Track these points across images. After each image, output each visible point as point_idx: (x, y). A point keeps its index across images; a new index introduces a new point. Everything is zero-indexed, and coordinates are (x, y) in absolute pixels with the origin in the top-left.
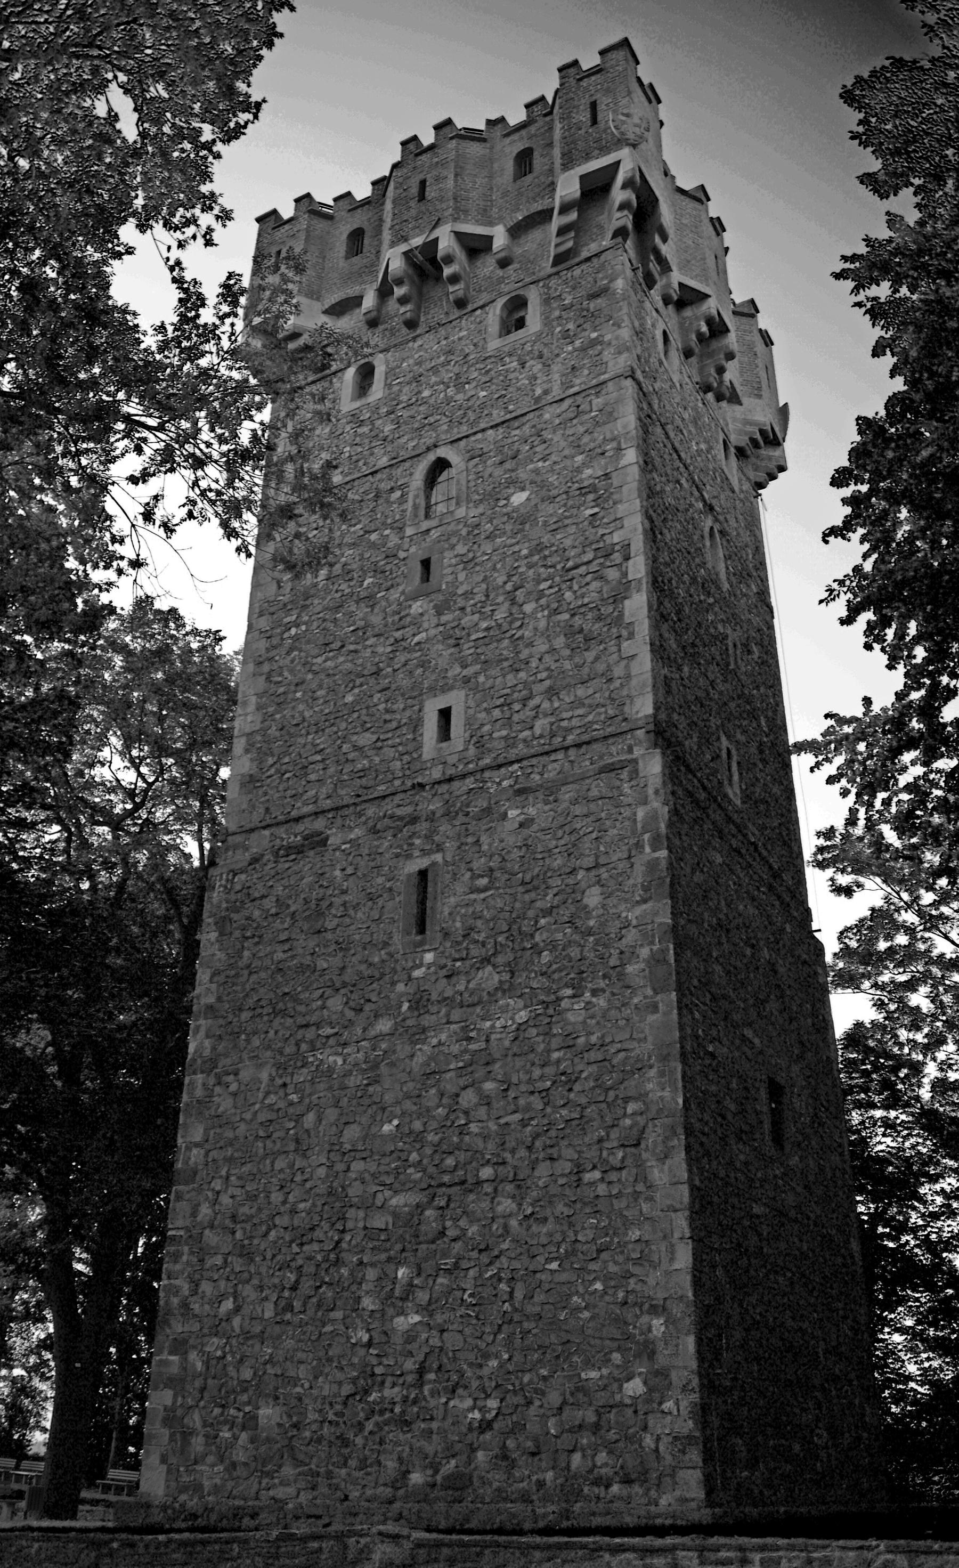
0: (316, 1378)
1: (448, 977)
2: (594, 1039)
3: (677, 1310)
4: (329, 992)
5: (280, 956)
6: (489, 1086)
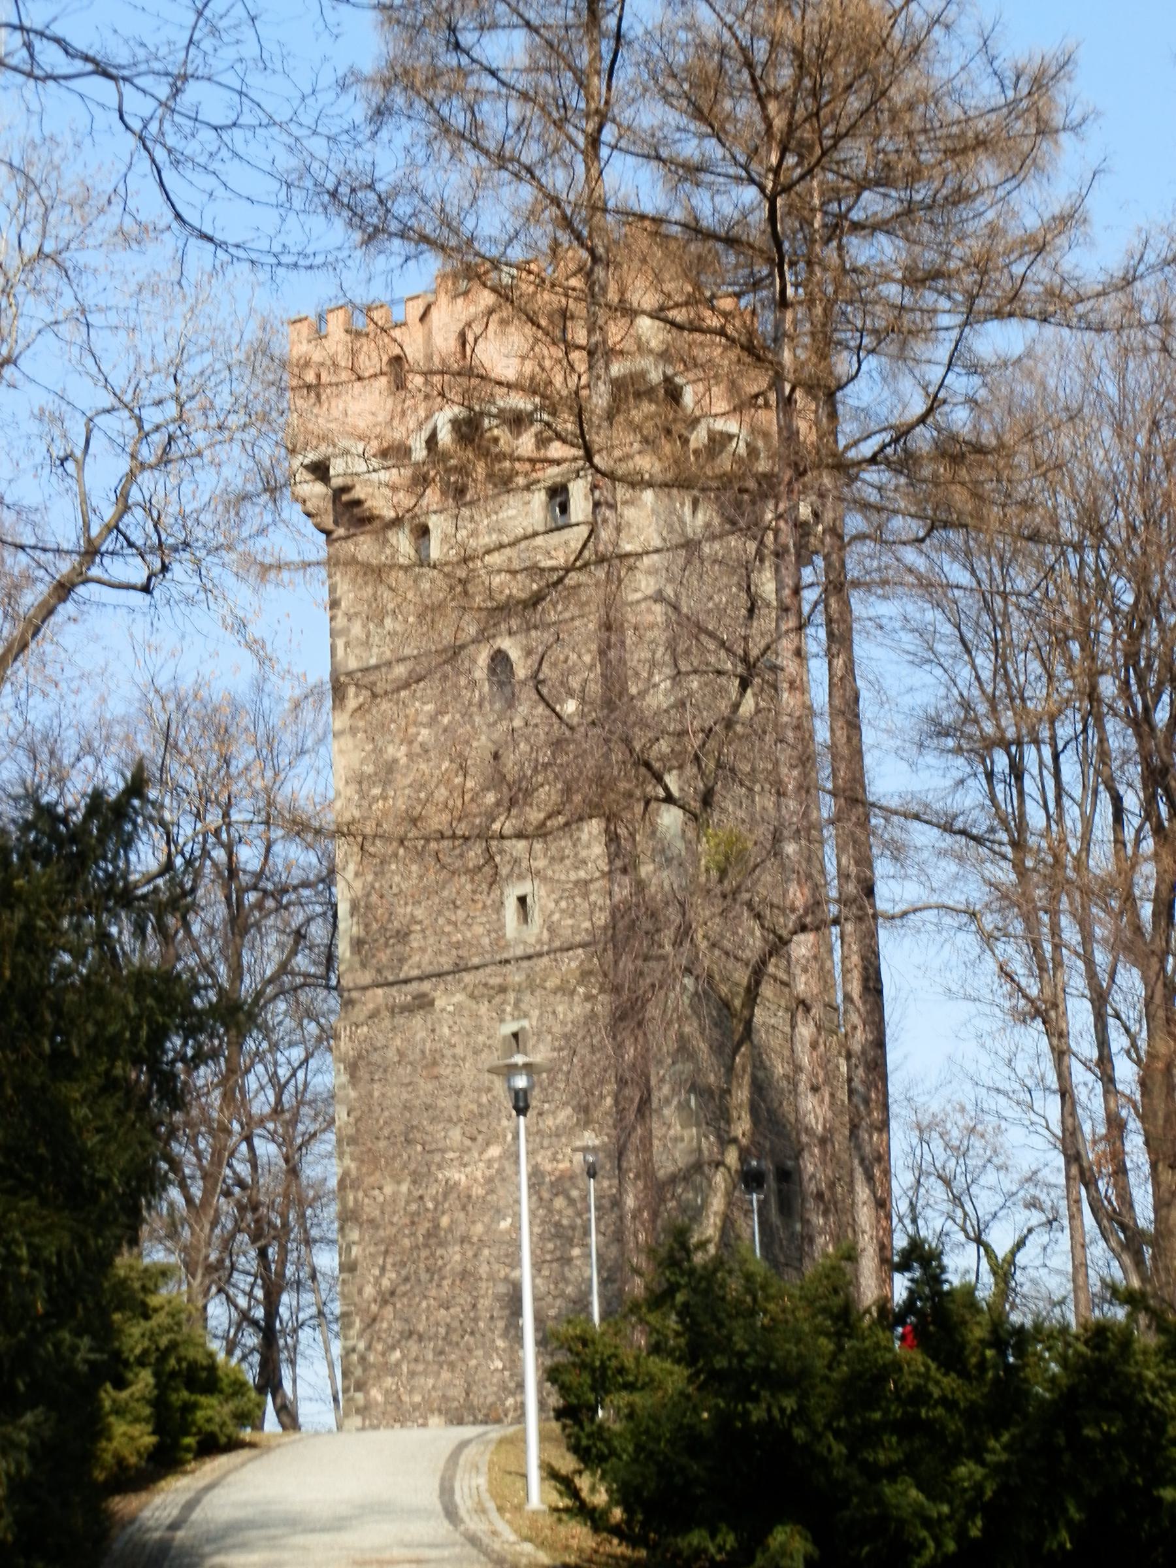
5: (405, 1096)
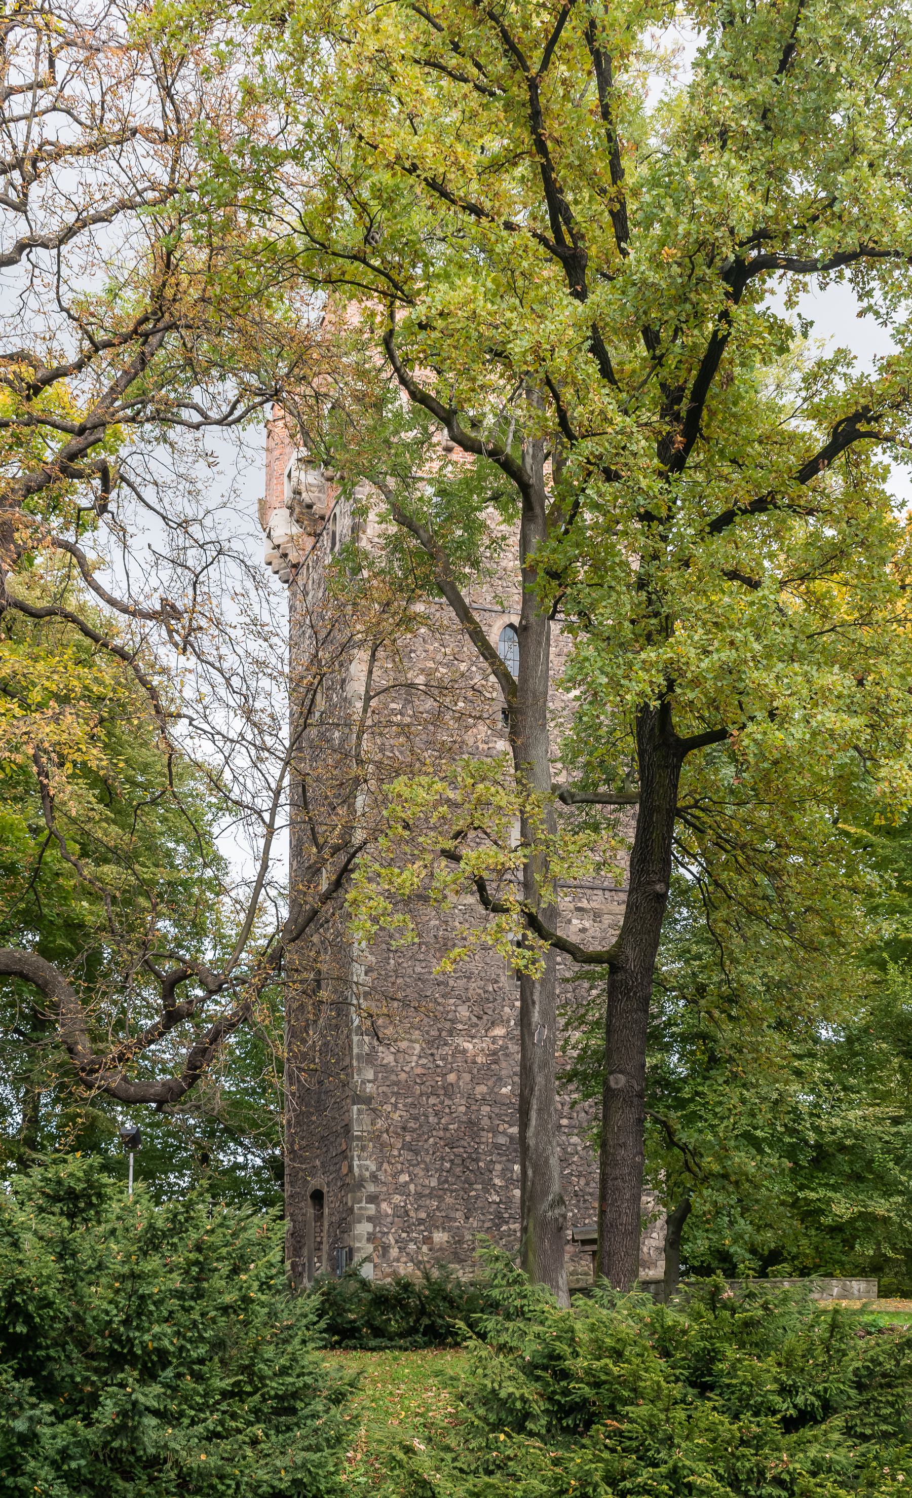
0: (467, 1218)
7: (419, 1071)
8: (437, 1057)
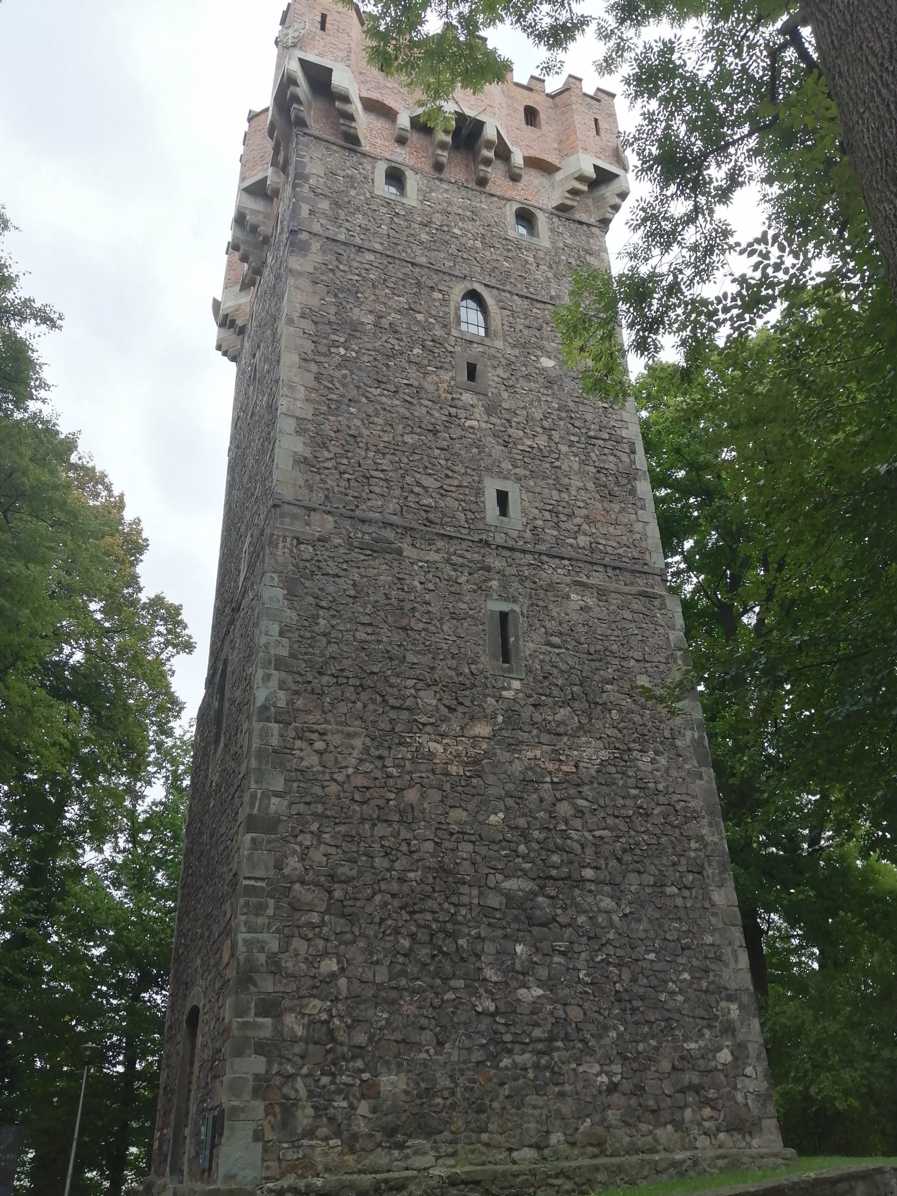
0: (440, 1044)
1: (535, 706)
2: (661, 787)
3: (745, 999)
4: (420, 685)
6: (581, 802)
7: (359, 781)
8: (389, 762)
